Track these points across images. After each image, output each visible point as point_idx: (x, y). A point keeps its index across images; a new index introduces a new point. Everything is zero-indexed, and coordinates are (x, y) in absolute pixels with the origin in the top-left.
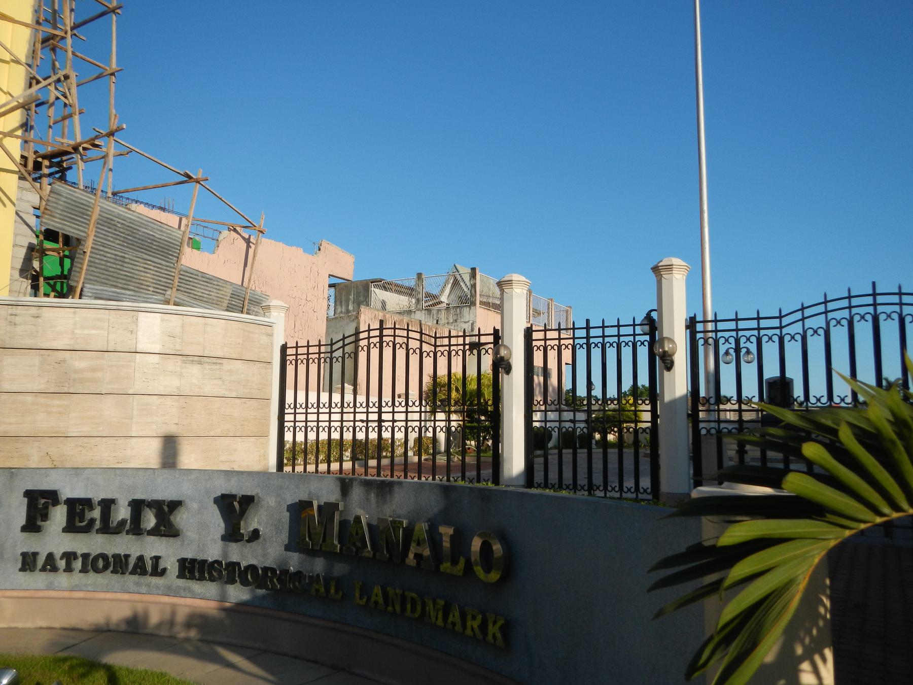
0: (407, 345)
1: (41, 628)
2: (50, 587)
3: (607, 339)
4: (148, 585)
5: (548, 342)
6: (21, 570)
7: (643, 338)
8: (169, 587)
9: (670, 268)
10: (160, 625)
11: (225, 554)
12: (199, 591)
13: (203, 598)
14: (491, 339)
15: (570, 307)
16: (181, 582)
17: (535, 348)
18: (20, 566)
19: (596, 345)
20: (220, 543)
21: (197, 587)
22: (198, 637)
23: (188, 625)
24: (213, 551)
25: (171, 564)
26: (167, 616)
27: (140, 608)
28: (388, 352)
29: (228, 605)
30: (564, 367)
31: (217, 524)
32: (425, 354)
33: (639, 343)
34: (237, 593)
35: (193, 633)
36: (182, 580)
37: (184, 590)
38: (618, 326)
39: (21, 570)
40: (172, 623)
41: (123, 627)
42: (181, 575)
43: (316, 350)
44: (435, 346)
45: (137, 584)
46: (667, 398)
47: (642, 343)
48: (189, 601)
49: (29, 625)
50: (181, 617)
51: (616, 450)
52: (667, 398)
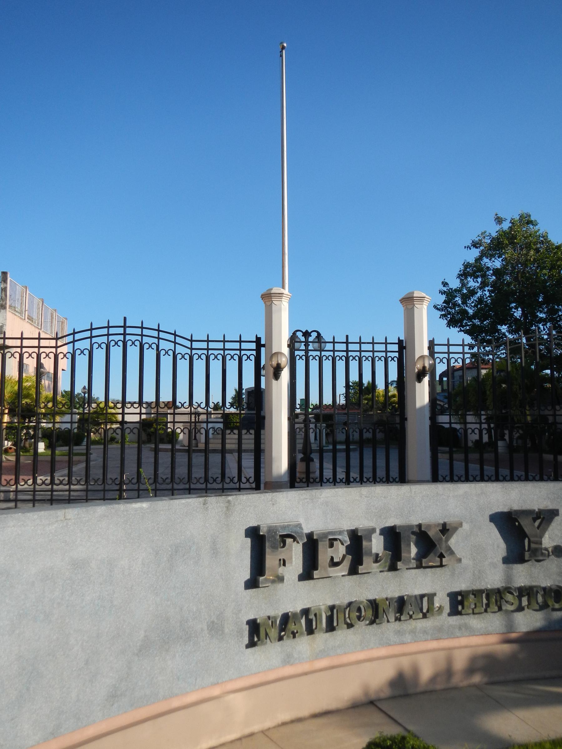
0: (158, 347)
1: (284, 724)
2: (288, 660)
3: (363, 354)
4: (413, 632)
5: (376, 354)
6: (248, 646)
7: (393, 355)
8: (440, 629)
9: (422, 299)
10: (433, 679)
11: (509, 577)
12: (479, 626)
13: (482, 634)
14: (253, 346)
15: (66, 319)
16: (455, 620)
17: (298, 358)
18: (246, 640)
19: (354, 358)
20: (501, 566)
21: (474, 622)
22: (486, 680)
23: (470, 670)
24: (494, 578)
25: (442, 601)
26: (442, 665)
27: (405, 663)
28: (133, 352)
29: (514, 635)
30: (60, 373)
31: (495, 544)
32: (179, 356)
33: (390, 359)
34: (528, 621)
35: (477, 679)
36: (455, 618)
37: (460, 628)
38: (360, 343)
39: (248, 646)
40: (449, 672)
41: (387, 693)
42: (454, 612)
43: (382, 347)
44: (192, 349)
45: (399, 633)
46: (418, 405)
47: (393, 359)
48: (464, 641)
49: (268, 724)
50: (460, 662)
51: (102, 446)
52: (418, 405)
